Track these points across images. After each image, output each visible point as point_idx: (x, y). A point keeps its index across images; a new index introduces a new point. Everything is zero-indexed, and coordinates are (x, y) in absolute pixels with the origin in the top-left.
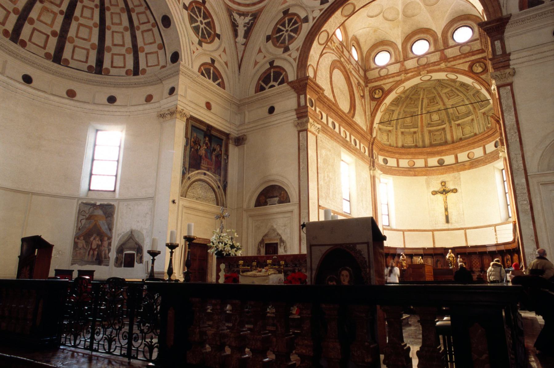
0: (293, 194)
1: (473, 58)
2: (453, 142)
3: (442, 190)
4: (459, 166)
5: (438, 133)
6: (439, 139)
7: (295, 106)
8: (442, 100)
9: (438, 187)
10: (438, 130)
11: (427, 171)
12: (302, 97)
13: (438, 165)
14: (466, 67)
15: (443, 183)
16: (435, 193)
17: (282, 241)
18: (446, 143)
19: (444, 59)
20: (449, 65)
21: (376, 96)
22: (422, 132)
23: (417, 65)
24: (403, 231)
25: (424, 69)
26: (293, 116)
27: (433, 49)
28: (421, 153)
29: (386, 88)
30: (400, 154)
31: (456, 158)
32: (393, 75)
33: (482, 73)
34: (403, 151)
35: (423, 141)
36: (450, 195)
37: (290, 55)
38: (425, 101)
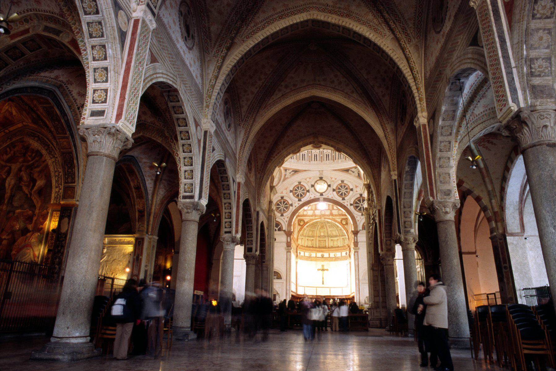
0: (283, 275)
1: (343, 217)
2: (329, 248)
3: (322, 269)
4: (330, 259)
5: (322, 242)
6: (323, 244)
7: (286, 241)
8: (327, 228)
9: (320, 268)
10: (322, 240)
11: (316, 259)
12: (289, 238)
13: (321, 256)
14: (339, 220)
15: (323, 266)
16: (319, 270)
17: (278, 293)
18: (325, 247)
19: (332, 214)
20: (333, 218)
21: (301, 224)
22: (316, 240)
23: (320, 214)
24: (305, 287)
25: (323, 216)
26: (285, 245)
27: (327, 208)
28: (315, 251)
29: (306, 221)
30: (306, 250)
31: (329, 255)
32: (309, 216)
33: (345, 225)
34: (307, 248)
35: (316, 245)
36: (325, 271)
37: (284, 219)
38: (319, 227)
